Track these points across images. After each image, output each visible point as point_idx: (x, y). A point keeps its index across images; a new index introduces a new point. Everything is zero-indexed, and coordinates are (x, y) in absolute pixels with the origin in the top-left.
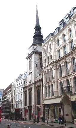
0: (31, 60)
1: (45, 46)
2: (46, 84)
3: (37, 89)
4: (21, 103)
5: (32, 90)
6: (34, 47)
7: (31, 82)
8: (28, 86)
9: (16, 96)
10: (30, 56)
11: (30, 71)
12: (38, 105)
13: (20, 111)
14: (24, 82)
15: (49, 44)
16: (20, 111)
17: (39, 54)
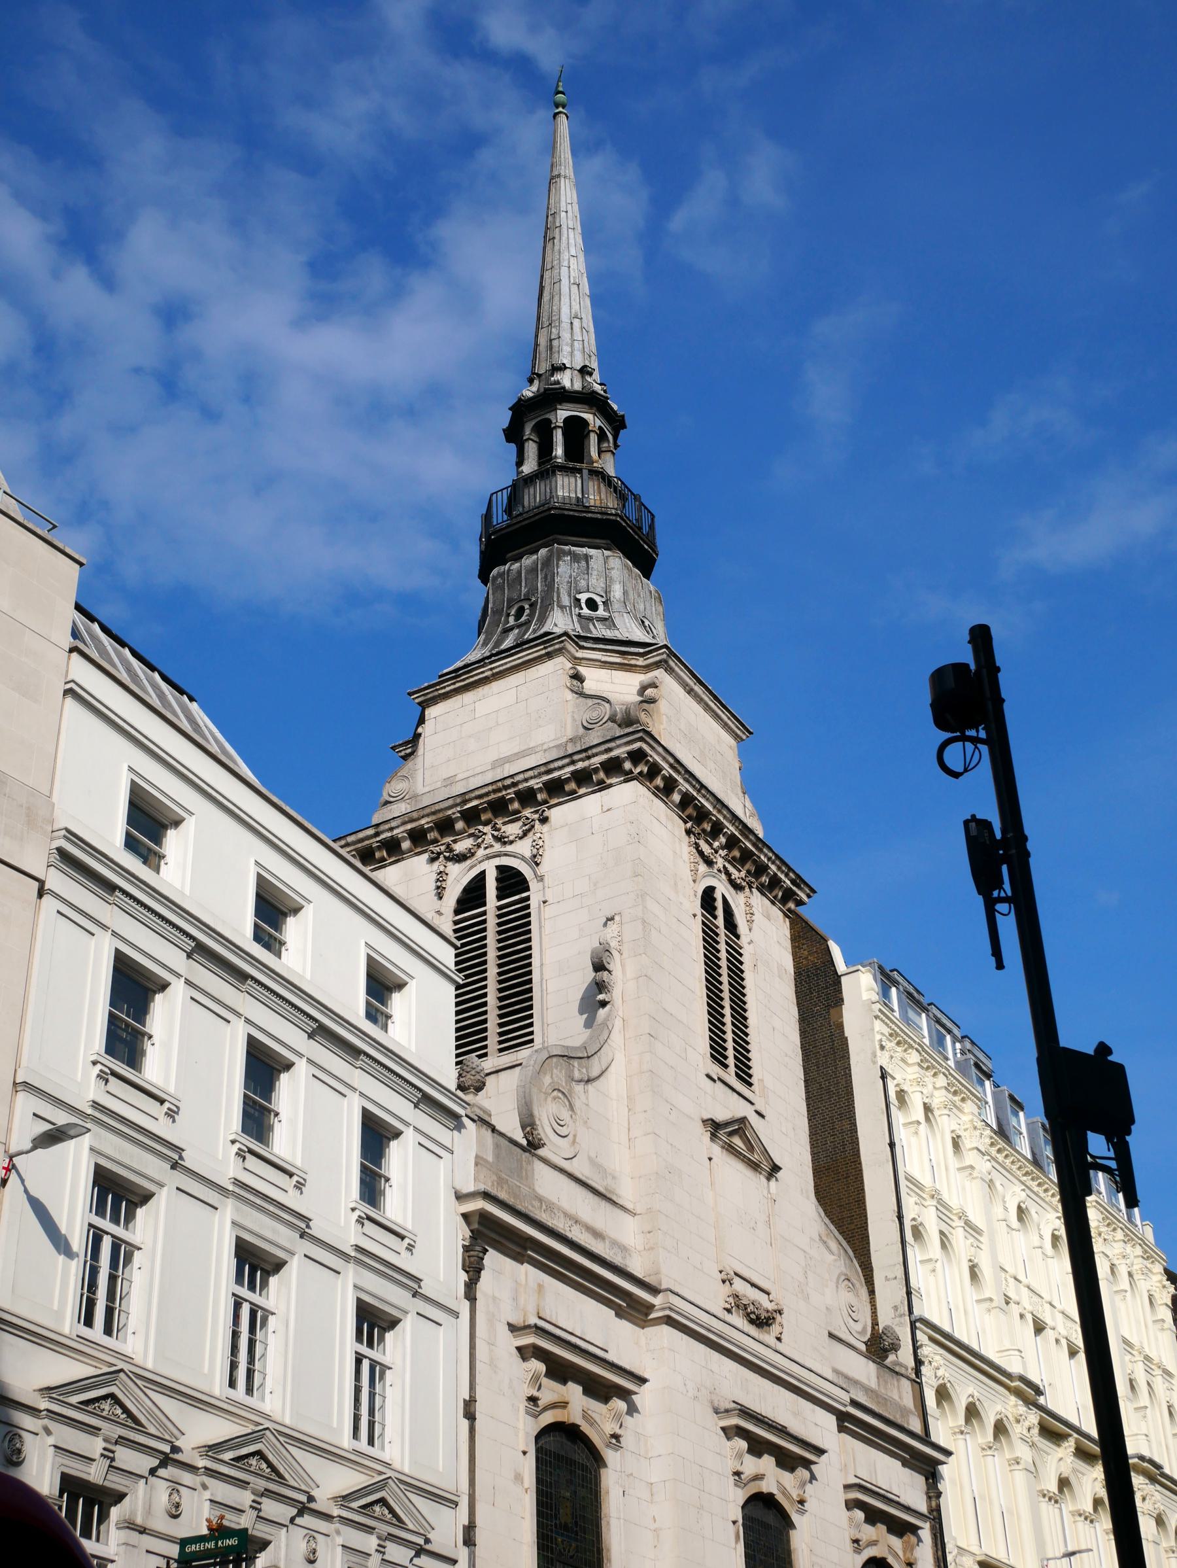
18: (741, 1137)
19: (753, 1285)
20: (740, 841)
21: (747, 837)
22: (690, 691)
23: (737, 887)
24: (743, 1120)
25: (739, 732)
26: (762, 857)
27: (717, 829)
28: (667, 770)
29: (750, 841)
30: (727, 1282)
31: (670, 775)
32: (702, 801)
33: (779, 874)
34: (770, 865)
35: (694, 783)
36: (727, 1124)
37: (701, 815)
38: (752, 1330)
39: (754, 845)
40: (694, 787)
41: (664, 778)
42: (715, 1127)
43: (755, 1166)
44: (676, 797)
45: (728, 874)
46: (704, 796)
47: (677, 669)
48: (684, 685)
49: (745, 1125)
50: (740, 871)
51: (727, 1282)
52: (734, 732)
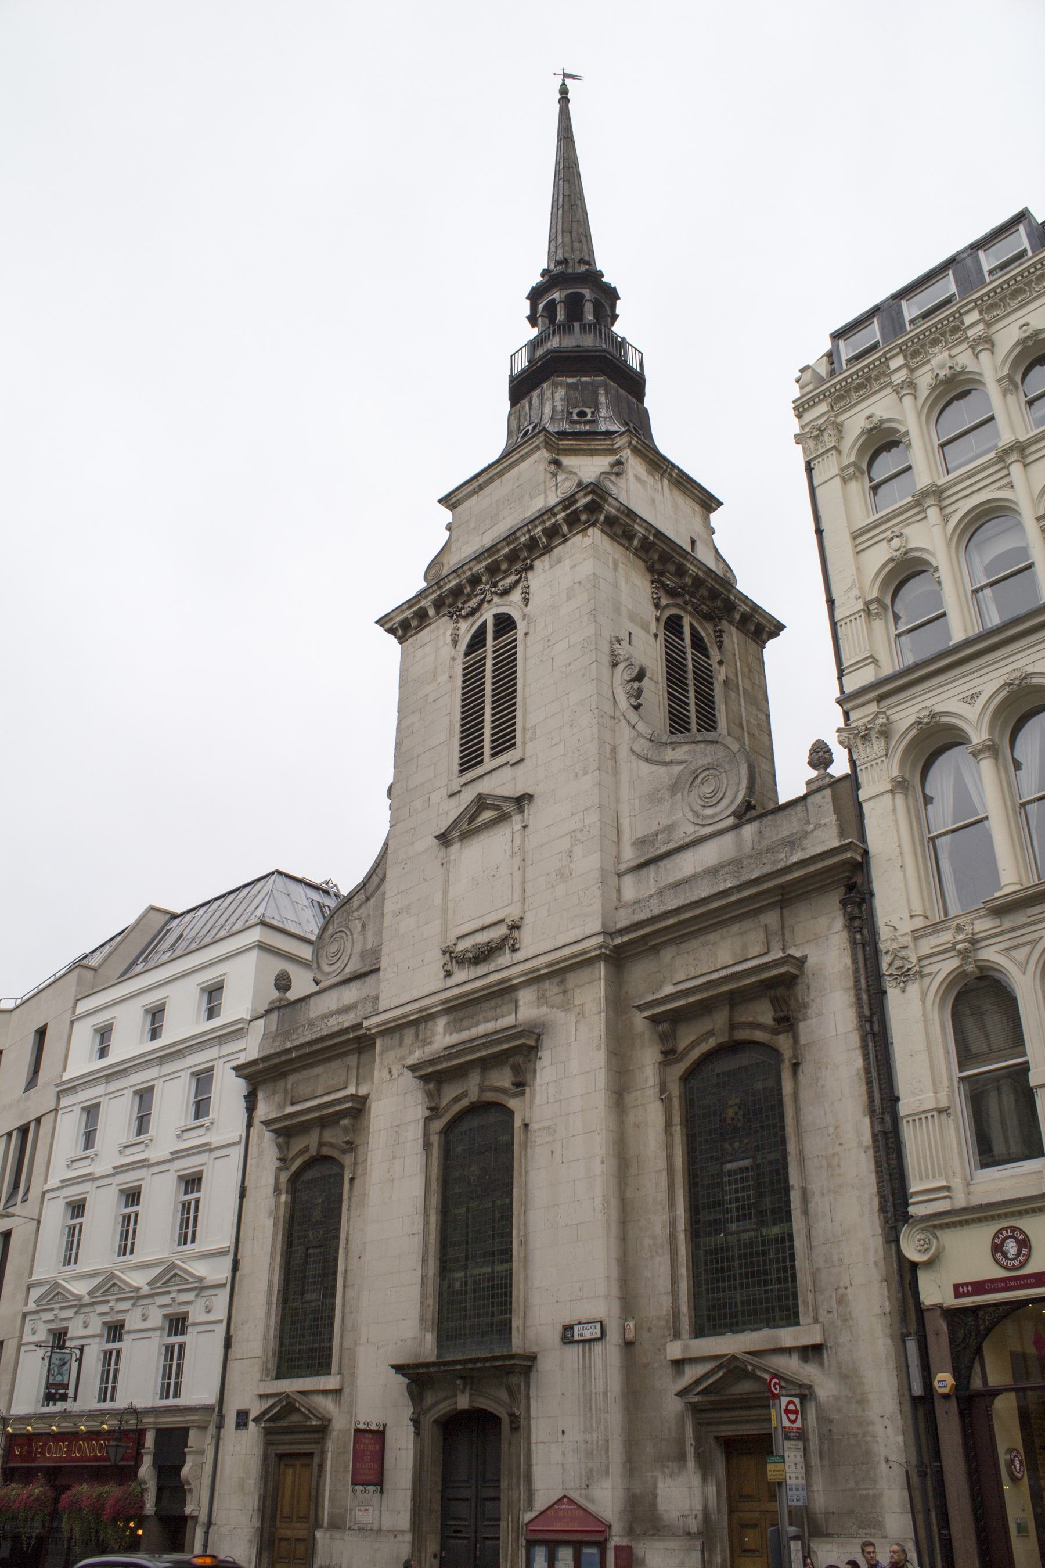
0: (505, 624)
1: (898, 378)
2: (984, 925)
3: (669, 1056)
4: (178, 1324)
5: (520, 1086)
6: (566, 461)
7: (483, 955)
8: (420, 1021)
9: (55, 1215)
10: (513, 557)
11: (485, 787)
12: (699, 1331)
13: (146, 1470)
14: (283, 983)
15: (987, 342)
16: (146, 1470)
17: (651, 569)
18: (488, 808)
19: (483, 929)
20: (495, 561)
21: (498, 551)
22: (481, 488)
23: (506, 592)
24: (480, 796)
25: (534, 445)
26: (522, 539)
27: (475, 580)
28: (408, 614)
29: (503, 548)
30: (447, 955)
31: (415, 612)
32: (447, 587)
33: (548, 524)
34: (532, 534)
35: (431, 590)
36: (456, 823)
37: (457, 592)
38: (482, 969)
39: (508, 544)
40: (434, 592)
41: (412, 618)
42: (444, 839)
43: (503, 818)
44: (431, 612)
45: (496, 593)
46: (446, 584)
47: (458, 497)
48: (475, 492)
49: (484, 798)
50: (511, 573)
51: (447, 955)
52: (532, 450)
